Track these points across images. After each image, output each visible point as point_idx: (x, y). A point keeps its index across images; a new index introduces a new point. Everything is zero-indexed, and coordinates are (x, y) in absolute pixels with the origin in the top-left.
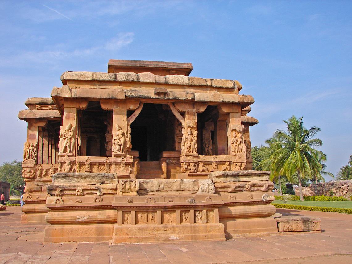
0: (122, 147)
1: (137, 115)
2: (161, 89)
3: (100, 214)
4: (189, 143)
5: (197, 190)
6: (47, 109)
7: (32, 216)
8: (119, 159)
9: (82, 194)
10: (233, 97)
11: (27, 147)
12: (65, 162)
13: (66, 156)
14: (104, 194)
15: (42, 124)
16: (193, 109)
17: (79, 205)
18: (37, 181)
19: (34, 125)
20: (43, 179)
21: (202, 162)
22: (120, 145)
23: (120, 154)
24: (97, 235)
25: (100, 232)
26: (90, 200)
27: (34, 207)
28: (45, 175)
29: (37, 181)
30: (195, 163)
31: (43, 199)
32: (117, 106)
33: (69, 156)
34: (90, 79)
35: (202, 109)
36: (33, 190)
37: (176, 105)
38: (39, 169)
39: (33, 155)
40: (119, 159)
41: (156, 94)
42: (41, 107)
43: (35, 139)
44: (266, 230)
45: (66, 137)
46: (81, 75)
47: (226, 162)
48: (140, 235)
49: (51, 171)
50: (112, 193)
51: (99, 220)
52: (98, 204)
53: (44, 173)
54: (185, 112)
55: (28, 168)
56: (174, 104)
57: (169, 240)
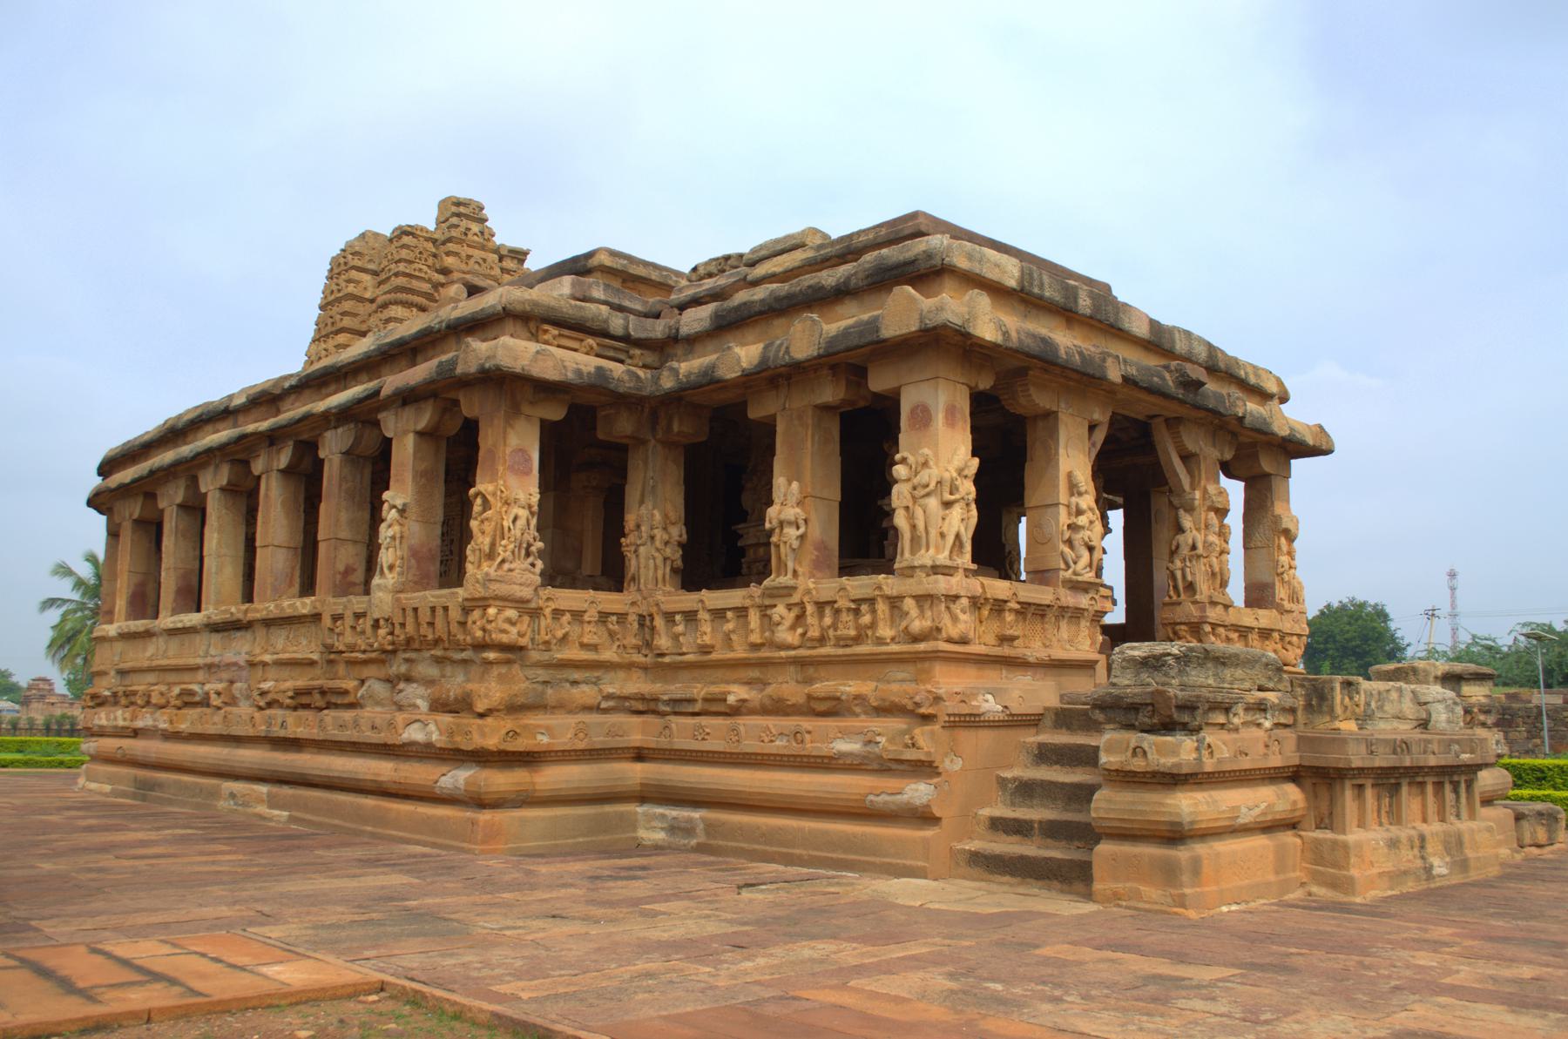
12: (957, 597)
15: (556, 413)
17: (1245, 764)
19: (526, 409)
27: (528, 779)
34: (1012, 283)
36: (521, 700)
38: (547, 611)
39: (529, 545)
45: (957, 496)
48: (1388, 867)
52: (1276, 761)
56: (1173, 423)
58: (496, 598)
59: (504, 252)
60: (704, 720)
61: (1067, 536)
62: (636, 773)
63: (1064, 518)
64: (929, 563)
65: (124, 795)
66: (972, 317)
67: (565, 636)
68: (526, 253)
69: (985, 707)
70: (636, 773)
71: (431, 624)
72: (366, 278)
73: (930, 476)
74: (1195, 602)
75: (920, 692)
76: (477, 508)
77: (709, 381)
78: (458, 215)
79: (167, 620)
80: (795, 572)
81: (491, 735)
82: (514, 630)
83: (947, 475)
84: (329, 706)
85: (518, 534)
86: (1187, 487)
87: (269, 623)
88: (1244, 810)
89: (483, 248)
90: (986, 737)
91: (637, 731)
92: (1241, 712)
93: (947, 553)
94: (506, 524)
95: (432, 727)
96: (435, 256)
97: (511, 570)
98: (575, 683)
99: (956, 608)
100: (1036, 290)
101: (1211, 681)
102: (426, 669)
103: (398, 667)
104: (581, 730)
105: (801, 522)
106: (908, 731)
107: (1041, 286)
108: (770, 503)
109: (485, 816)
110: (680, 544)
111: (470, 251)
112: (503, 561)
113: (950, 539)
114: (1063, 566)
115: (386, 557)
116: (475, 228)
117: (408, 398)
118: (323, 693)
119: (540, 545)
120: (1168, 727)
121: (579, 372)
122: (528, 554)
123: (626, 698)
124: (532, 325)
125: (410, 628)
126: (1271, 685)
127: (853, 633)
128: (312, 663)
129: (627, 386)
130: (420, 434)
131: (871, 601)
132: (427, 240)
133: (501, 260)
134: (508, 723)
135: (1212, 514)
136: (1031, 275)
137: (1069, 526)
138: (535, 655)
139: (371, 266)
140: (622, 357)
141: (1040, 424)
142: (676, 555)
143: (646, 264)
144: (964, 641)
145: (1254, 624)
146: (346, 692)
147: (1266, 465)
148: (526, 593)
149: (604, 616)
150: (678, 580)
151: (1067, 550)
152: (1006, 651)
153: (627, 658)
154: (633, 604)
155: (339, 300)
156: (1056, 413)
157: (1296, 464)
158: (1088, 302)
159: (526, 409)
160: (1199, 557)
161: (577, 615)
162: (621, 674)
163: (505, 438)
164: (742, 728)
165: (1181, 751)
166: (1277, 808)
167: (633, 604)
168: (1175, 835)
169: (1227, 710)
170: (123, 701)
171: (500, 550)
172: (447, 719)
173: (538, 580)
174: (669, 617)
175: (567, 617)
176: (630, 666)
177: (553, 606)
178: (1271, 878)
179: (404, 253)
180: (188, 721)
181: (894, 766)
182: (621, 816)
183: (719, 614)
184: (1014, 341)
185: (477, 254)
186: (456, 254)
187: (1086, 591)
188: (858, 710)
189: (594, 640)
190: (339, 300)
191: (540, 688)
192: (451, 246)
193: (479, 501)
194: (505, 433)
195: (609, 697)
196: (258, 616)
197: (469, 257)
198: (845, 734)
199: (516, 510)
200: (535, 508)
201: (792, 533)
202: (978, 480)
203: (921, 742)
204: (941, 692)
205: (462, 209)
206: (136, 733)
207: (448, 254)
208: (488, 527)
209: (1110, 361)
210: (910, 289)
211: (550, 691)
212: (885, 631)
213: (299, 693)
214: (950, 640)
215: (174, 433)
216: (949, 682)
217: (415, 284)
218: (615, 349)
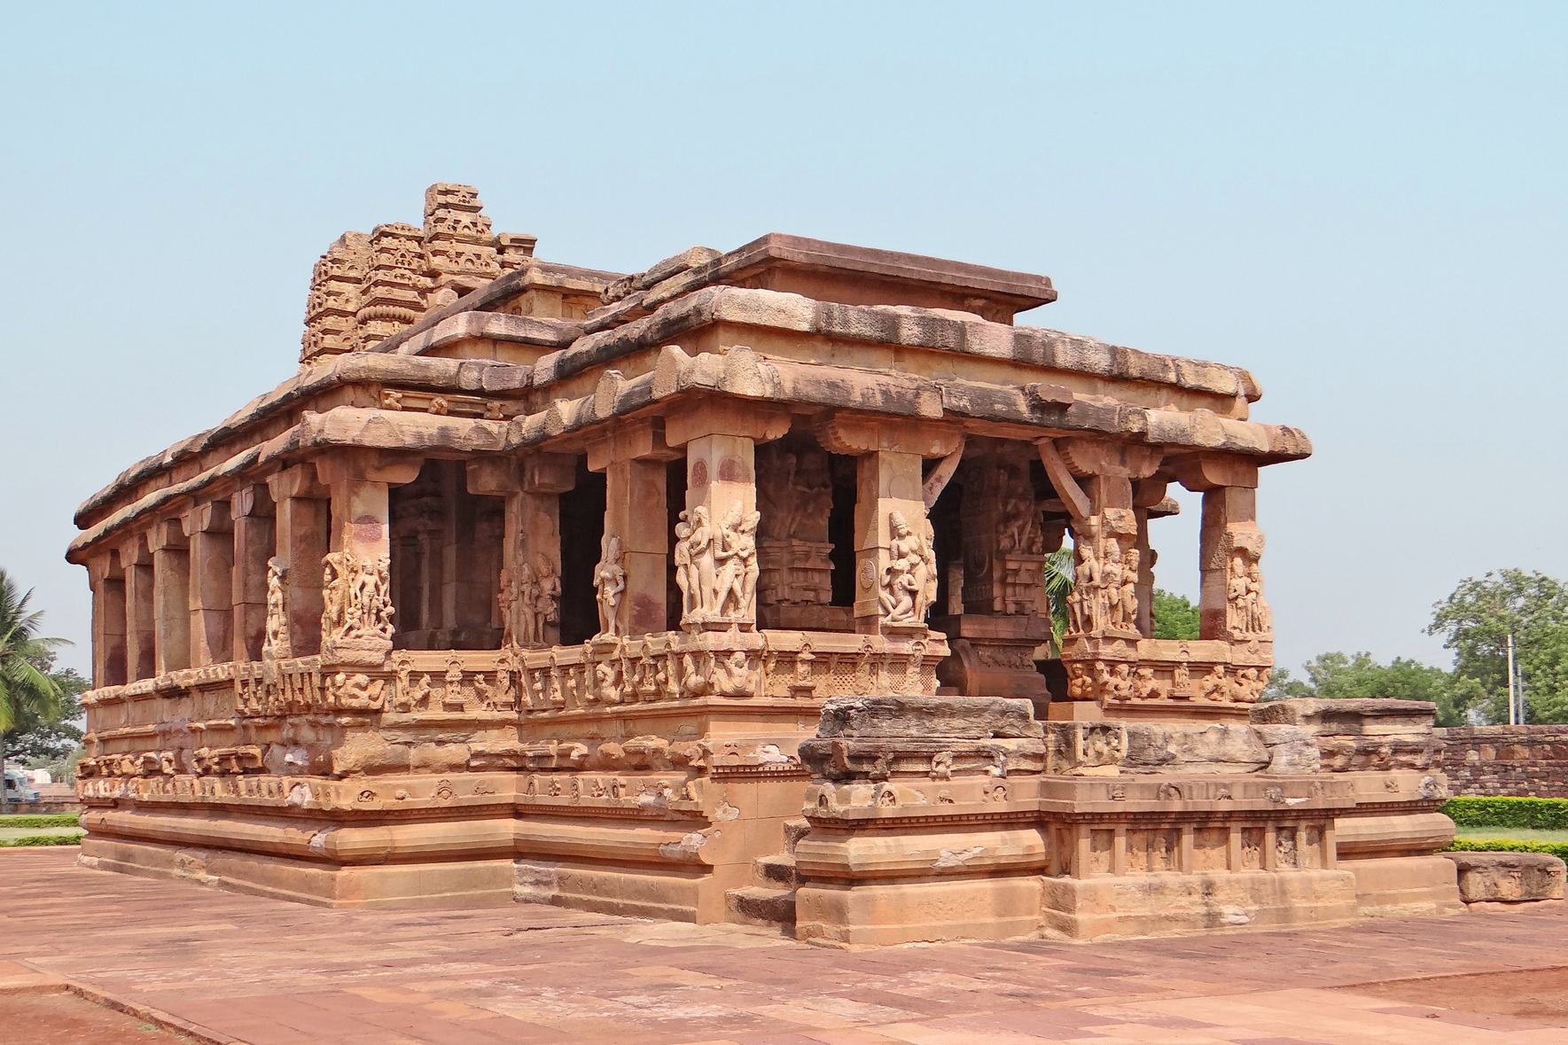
1: (946, 481)
3: (1004, 842)
6: (425, 410)
7: (383, 876)
8: (906, 647)
12: (729, 653)
15: (406, 476)
17: (947, 810)
19: (372, 475)
22: (913, 594)
24: (999, 915)
25: (1006, 906)
28: (424, 701)
32: (892, 443)
33: (744, 628)
34: (805, 327)
36: (378, 762)
39: (379, 611)
40: (906, 647)
41: (1039, 405)
44: (1432, 896)
46: (781, 311)
48: (1144, 911)
52: (1001, 806)
57: (1222, 925)
58: (344, 664)
59: (505, 242)
60: (555, 777)
61: (887, 579)
62: (507, 829)
63: (884, 561)
64: (700, 620)
65: (105, 866)
66: (730, 374)
67: (426, 698)
68: (533, 242)
69: (763, 758)
70: (507, 829)
71: (301, 690)
72: (348, 288)
73: (702, 536)
74: (1090, 639)
75: (688, 748)
76: (327, 577)
77: (543, 437)
78: (446, 206)
79: (133, 687)
80: (617, 628)
81: (346, 796)
82: (364, 695)
83: (718, 533)
84: (246, 772)
85: (366, 601)
86: (1084, 511)
87: (205, 688)
88: (944, 853)
89: (477, 242)
90: (771, 788)
91: (507, 787)
92: (949, 762)
93: (717, 609)
94: (352, 592)
95: (306, 789)
96: (421, 256)
98: (440, 743)
99: (730, 663)
100: (838, 329)
101: (913, 732)
102: (307, 734)
103: (287, 733)
104: (444, 788)
106: (684, 785)
107: (846, 323)
108: (596, 556)
109: (345, 872)
110: (553, 598)
111: (461, 247)
112: (351, 628)
113: (723, 595)
114: (881, 612)
115: (274, 623)
116: (466, 218)
117: (284, 462)
118: (239, 758)
119: (390, 609)
120: (847, 777)
121: (420, 436)
122: (379, 619)
123: (499, 756)
125: (289, 694)
126: (1015, 732)
127: (653, 688)
128: (232, 729)
129: (478, 442)
130: (297, 499)
131: (663, 657)
132: (409, 238)
133: (501, 251)
135: (1114, 541)
136: (830, 316)
137: (889, 571)
138: (390, 717)
139: (352, 274)
141: (867, 464)
142: (551, 610)
143: (589, 275)
144: (741, 694)
145: (1183, 658)
146: (253, 758)
147: (1213, 476)
148: (377, 657)
149: (468, 678)
150: (554, 634)
151: (884, 594)
152: (801, 702)
154: (502, 661)
155: (320, 316)
158: (916, 330)
159: (372, 475)
160: (1097, 588)
161: (438, 677)
162: (495, 733)
163: (349, 507)
164: (580, 784)
165: (859, 798)
166: (998, 853)
167: (502, 661)
168: (851, 879)
169: (929, 758)
170: (105, 771)
171: (347, 617)
172: (317, 780)
173: (390, 643)
174: (531, 671)
175: (427, 678)
176: (502, 724)
177: (409, 668)
178: (991, 920)
179: (384, 259)
180: (148, 791)
181: (680, 817)
183: (564, 669)
184: (788, 391)
185: (470, 249)
186: (443, 253)
188: (658, 763)
189: (460, 699)
190: (320, 316)
191: (401, 748)
192: (438, 245)
193: (328, 571)
194: (349, 500)
195: (476, 755)
196: (192, 682)
197: (459, 254)
198: (648, 787)
199: (362, 577)
200: (386, 573)
201: (610, 591)
202: (762, 533)
203: (693, 794)
204: (709, 745)
205: (450, 199)
206: (116, 804)
207: (435, 253)
208: (336, 596)
209: (925, 396)
210: (676, 350)
211: (413, 751)
212: (674, 687)
213: (224, 759)
214: (724, 694)
215: (125, 491)
216: (722, 737)
217: (398, 294)
218: (471, 403)
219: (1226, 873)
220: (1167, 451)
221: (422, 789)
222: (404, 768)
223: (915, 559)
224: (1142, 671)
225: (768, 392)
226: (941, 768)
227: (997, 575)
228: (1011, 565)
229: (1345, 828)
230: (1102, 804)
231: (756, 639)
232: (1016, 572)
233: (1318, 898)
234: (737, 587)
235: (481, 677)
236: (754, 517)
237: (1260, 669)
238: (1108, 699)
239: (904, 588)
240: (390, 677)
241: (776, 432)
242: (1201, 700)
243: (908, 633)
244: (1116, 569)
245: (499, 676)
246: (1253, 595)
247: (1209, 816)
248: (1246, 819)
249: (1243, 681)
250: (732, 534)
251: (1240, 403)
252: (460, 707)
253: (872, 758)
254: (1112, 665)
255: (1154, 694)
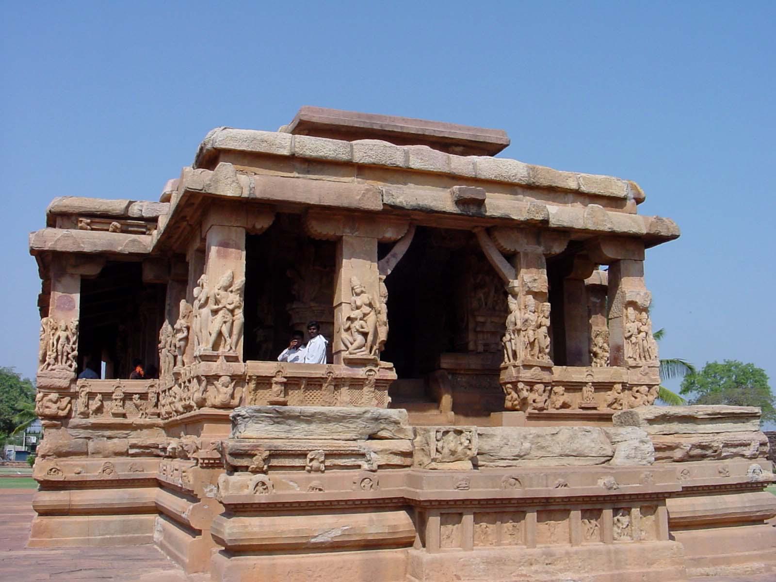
0: (370, 338)
1: (400, 256)
2: (471, 192)
3: (371, 521)
4: (531, 333)
5: (610, 454)
6: (107, 230)
8: (361, 372)
9: (322, 467)
10: (634, 221)
11: (49, 330)
12: (217, 377)
13: (221, 360)
14: (380, 467)
15: (92, 271)
16: (537, 246)
18: (76, 427)
20: (92, 420)
21: (558, 383)
22: (365, 335)
23: (365, 357)
26: (343, 484)
28: (99, 410)
29: (76, 427)
30: (546, 384)
31: (96, 476)
33: (229, 359)
35: (558, 249)
36: (65, 449)
37: (496, 234)
38: (83, 394)
39: (69, 354)
40: (361, 372)
41: (460, 202)
42: (92, 222)
43: (70, 310)
45: (220, 306)
47: (615, 383)
49: (116, 400)
50: (399, 463)
51: (370, 538)
53: (94, 404)
54: (519, 253)
55: (54, 388)
82: (54, 406)
83: (211, 294)
85: (60, 347)
97: (52, 370)
98: (109, 438)
105: (185, 329)
112: (49, 364)
113: (214, 335)
114: (343, 347)
122: (68, 359)
123: (147, 447)
124: (73, 218)
134: (51, 463)
135: (531, 297)
137: (349, 319)
138: (74, 421)
140: (144, 230)
145: (589, 379)
148: (64, 383)
149: (128, 396)
153: (148, 421)
154: (152, 386)
156: (342, 237)
157: (648, 252)
160: (519, 331)
161: (107, 396)
171: (47, 359)
173: (73, 375)
175: (99, 397)
176: (150, 426)
177: (87, 390)
182: (141, 522)
187: (365, 365)
189: (121, 410)
195: (133, 446)
199: (60, 333)
219: (567, 547)
220: (573, 237)
221: (92, 468)
222: (86, 454)
223: (366, 309)
224: (556, 389)
225: (246, 194)
226: (315, 464)
227: (471, 326)
228: (480, 319)
229: (678, 506)
230: (450, 493)
231: (240, 367)
232: (484, 323)
233: (650, 564)
234: (225, 330)
235: (137, 396)
236: (240, 280)
237: (650, 386)
238: (530, 410)
239: (358, 331)
240: (75, 396)
241: (263, 223)
242: (603, 409)
243: (362, 363)
244: (532, 317)
245: (150, 395)
246: (643, 334)
247: (547, 501)
248: (586, 503)
249: (637, 395)
250: (222, 293)
251: (630, 203)
252: (124, 416)
253: (248, 454)
254: (531, 385)
255: (565, 405)
